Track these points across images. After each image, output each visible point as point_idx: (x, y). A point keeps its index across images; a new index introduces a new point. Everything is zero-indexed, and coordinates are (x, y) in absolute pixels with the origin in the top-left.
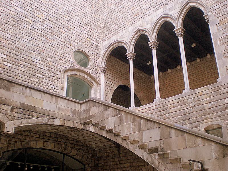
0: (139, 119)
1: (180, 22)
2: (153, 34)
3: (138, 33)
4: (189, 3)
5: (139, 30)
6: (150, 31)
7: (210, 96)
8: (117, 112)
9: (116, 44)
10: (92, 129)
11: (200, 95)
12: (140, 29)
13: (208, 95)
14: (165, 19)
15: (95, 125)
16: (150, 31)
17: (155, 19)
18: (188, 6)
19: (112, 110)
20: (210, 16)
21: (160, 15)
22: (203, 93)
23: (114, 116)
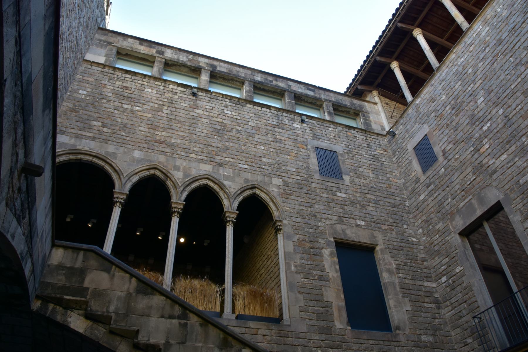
0: (237, 346)
1: (236, 204)
2: (182, 192)
3: (152, 172)
4: (255, 188)
5: (155, 168)
6: (180, 185)
7: (270, 341)
8: (177, 311)
9: (90, 158)
10: (77, 323)
11: (254, 333)
12: (159, 167)
13: (269, 338)
14: (211, 184)
15: (89, 316)
16: (180, 185)
17: (194, 173)
18: (253, 191)
19: (164, 302)
20: (285, 224)
21: (204, 173)
22: (260, 332)
23: (167, 316)
